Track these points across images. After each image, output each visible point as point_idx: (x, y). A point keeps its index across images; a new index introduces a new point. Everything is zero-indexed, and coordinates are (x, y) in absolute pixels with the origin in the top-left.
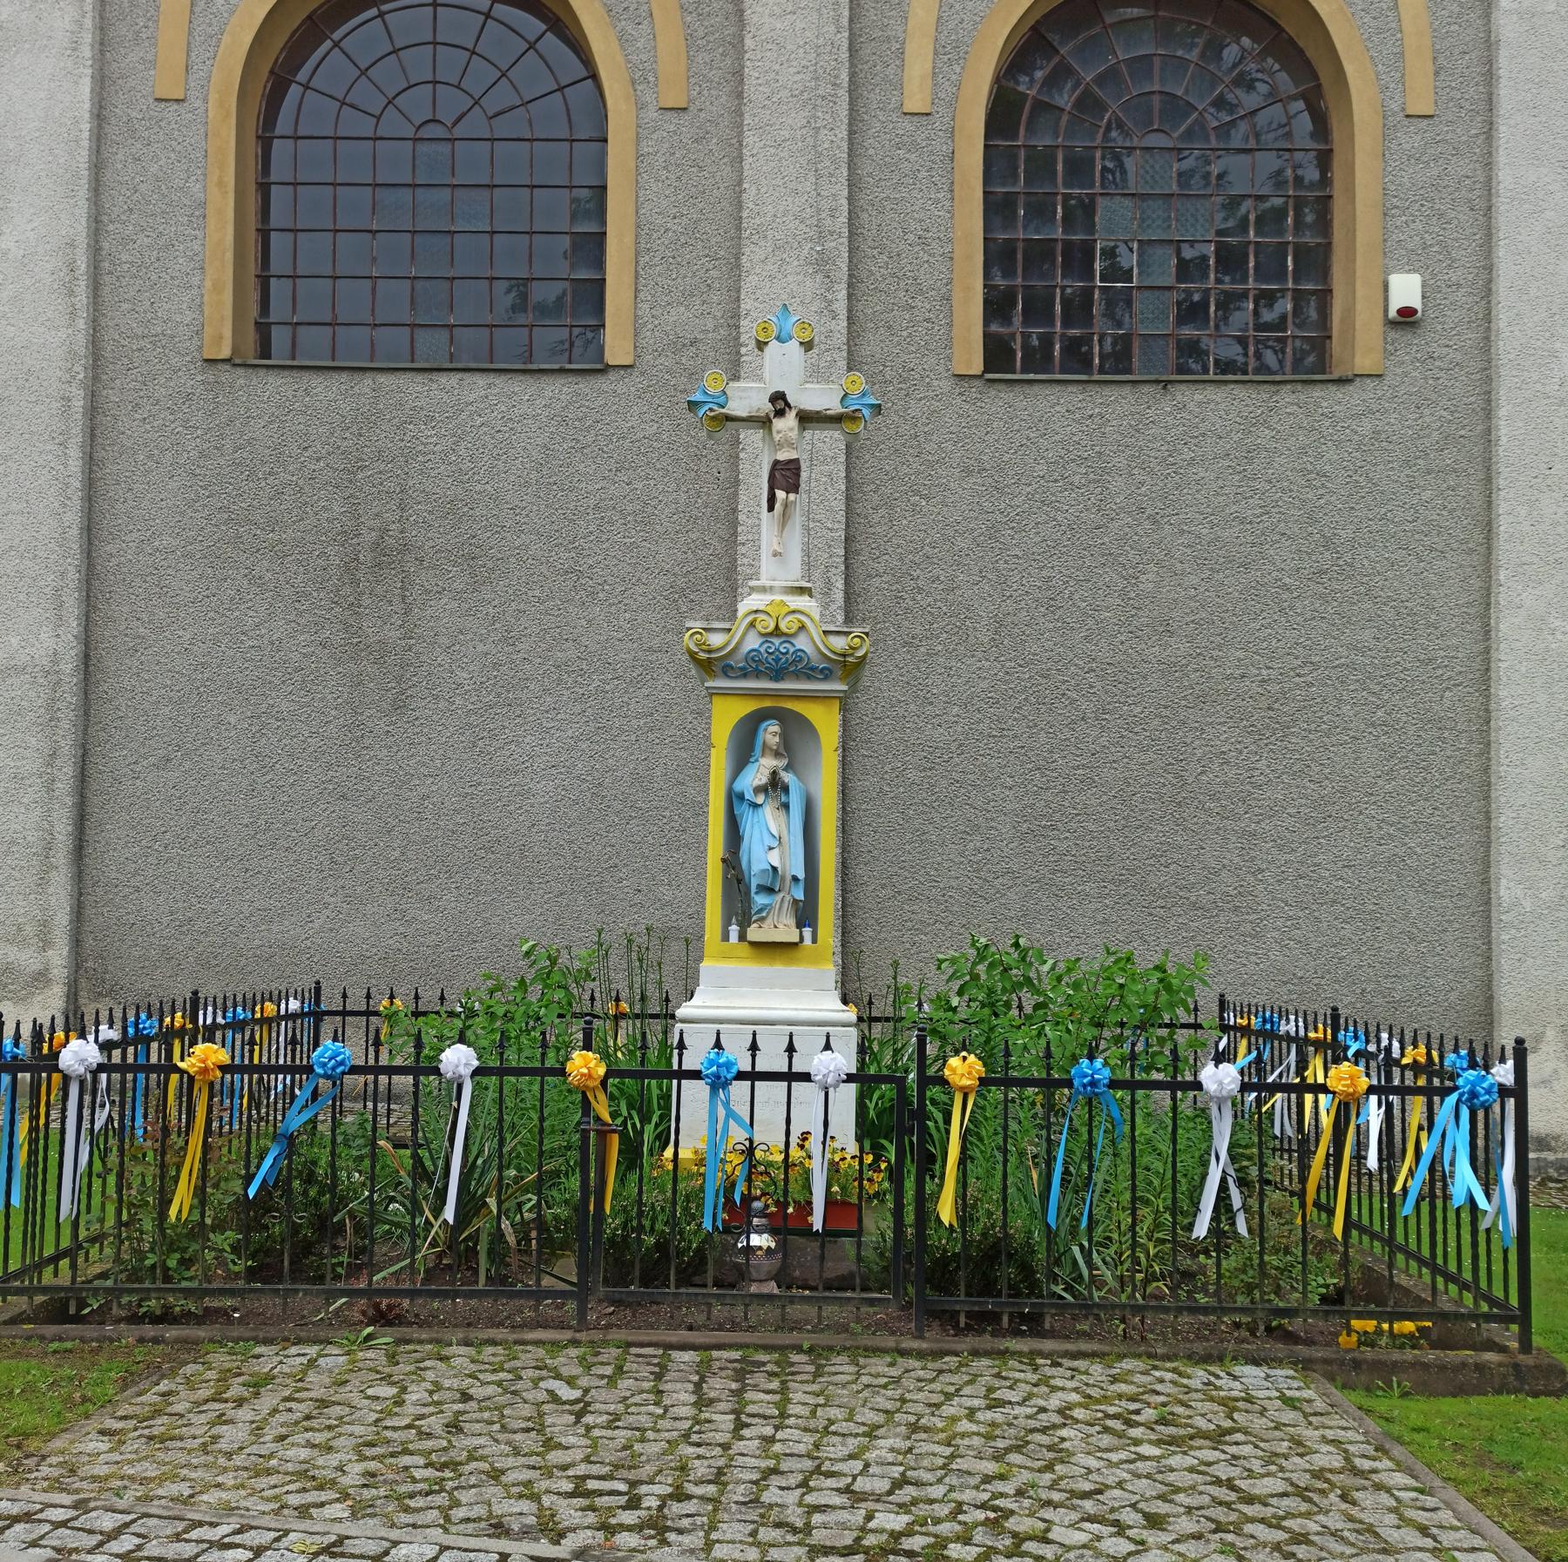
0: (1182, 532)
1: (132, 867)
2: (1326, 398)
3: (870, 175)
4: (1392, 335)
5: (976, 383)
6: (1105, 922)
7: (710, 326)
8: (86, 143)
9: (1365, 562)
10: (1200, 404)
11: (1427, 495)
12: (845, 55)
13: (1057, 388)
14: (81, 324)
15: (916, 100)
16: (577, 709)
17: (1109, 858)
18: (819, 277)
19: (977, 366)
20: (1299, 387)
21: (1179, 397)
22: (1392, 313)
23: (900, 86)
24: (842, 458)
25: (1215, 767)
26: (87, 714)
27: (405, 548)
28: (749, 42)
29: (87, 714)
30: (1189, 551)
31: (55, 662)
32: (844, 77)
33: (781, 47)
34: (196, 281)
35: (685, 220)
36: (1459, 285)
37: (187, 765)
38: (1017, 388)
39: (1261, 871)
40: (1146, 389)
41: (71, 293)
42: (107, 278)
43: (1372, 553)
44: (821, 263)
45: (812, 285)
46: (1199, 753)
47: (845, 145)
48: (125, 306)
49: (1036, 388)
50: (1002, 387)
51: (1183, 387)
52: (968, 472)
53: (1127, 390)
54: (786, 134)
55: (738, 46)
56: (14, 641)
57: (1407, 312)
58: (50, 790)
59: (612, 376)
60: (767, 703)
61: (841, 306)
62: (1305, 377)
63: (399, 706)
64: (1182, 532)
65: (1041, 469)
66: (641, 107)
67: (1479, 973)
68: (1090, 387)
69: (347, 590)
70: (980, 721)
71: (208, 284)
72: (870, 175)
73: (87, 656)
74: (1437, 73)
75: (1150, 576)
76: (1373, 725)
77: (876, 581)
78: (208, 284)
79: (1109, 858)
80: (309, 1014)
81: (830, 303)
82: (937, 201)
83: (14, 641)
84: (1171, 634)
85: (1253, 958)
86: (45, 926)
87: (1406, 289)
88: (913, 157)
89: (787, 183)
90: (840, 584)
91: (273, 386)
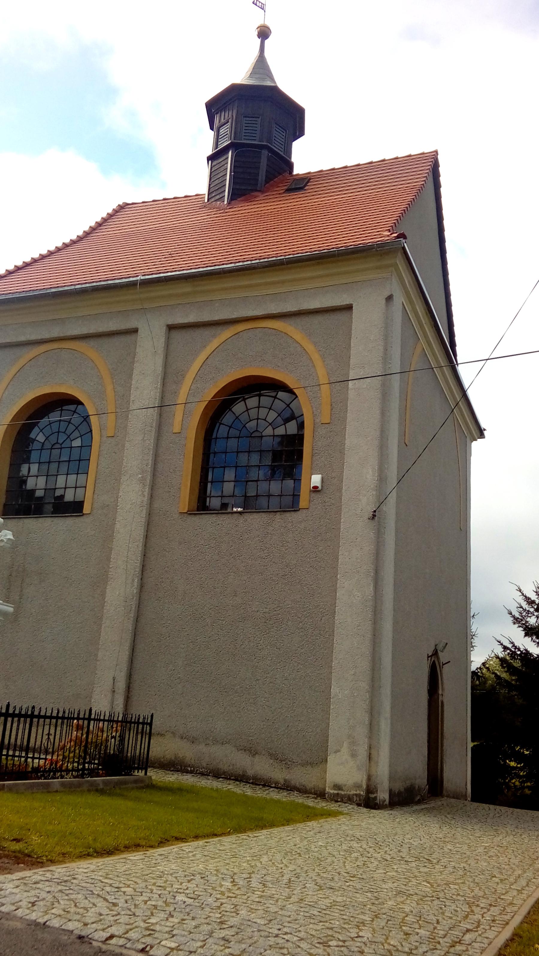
0: (242, 562)
2: (290, 517)
3: (162, 452)
4: (313, 495)
5: (186, 515)
9: (299, 572)
15: (177, 429)
18: (141, 484)
20: (282, 513)
21: (245, 518)
30: (244, 568)
35: (110, 469)
38: (198, 516)
44: (142, 481)
49: (203, 516)
50: (193, 516)
51: (247, 514)
54: (136, 442)
59: (85, 516)
62: (284, 510)
64: (242, 562)
68: (219, 515)
72: (162, 452)
81: (143, 492)
85: (253, 712)
87: (316, 480)
89: (135, 456)
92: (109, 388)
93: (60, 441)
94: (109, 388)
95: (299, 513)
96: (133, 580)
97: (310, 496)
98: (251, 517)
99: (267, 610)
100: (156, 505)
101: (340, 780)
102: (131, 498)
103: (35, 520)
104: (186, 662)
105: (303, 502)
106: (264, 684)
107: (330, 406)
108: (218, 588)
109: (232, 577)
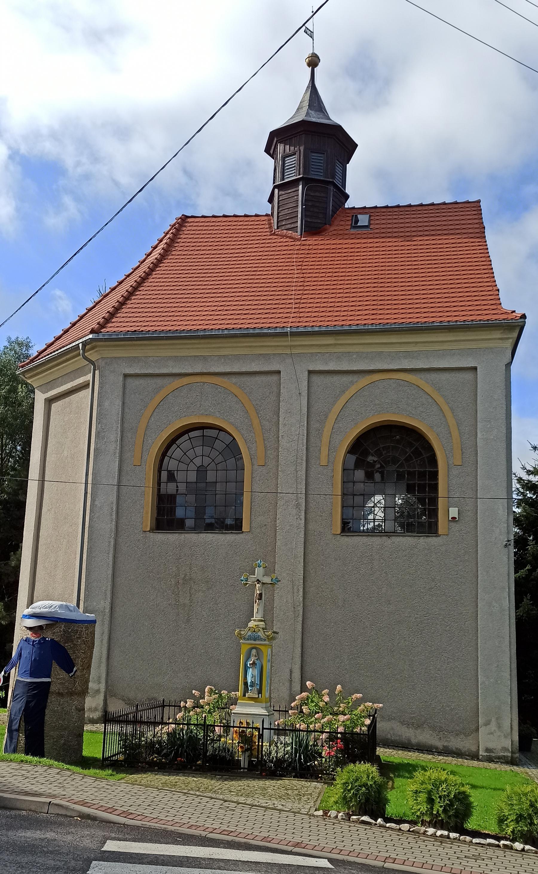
1: (121, 662)
2: (432, 540)
5: (339, 536)
6: (372, 684)
7: (269, 521)
8: (116, 478)
10: (398, 542)
11: (460, 568)
12: (305, 452)
13: (360, 537)
14: (114, 523)
16: (233, 622)
17: (374, 666)
19: (339, 531)
20: (425, 537)
22: (450, 519)
23: (319, 459)
24: (303, 557)
25: (402, 641)
26: (111, 622)
27: (191, 579)
28: (280, 449)
29: (111, 622)
31: (104, 609)
32: (305, 458)
33: (288, 450)
34: (142, 511)
36: (469, 511)
37: (135, 636)
39: (415, 671)
40: (384, 538)
41: (112, 515)
42: (120, 511)
43: (445, 583)
45: (294, 512)
46: (398, 637)
47: (304, 476)
48: (124, 518)
51: (394, 537)
52: (336, 560)
53: (379, 538)
55: (278, 449)
56: (95, 604)
57: (454, 518)
58: (102, 642)
59: (244, 534)
60: (253, 646)
61: (303, 517)
63: (188, 621)
65: (356, 559)
66: (253, 465)
67: (475, 701)
69: (176, 590)
70: (339, 627)
71: (145, 512)
73: (112, 607)
74: (462, 454)
75: (385, 588)
76: (446, 631)
77: (312, 589)
78: (145, 512)
79: (374, 666)
80: (161, 706)
82: (329, 488)
83: (95, 604)
84: (391, 604)
86: (99, 677)
87: (454, 512)
88: (323, 477)
90: (301, 590)
91: (160, 537)
92: (256, 422)
93: (205, 464)
94: (256, 422)
95: (439, 538)
96: (298, 590)
97: (449, 525)
98: (398, 540)
99: (418, 616)
100: (310, 527)
101: (491, 746)
102: (289, 521)
103: (196, 535)
104: (350, 657)
105: (441, 529)
106: (420, 674)
107: (460, 451)
108: (373, 597)
109: (385, 588)
